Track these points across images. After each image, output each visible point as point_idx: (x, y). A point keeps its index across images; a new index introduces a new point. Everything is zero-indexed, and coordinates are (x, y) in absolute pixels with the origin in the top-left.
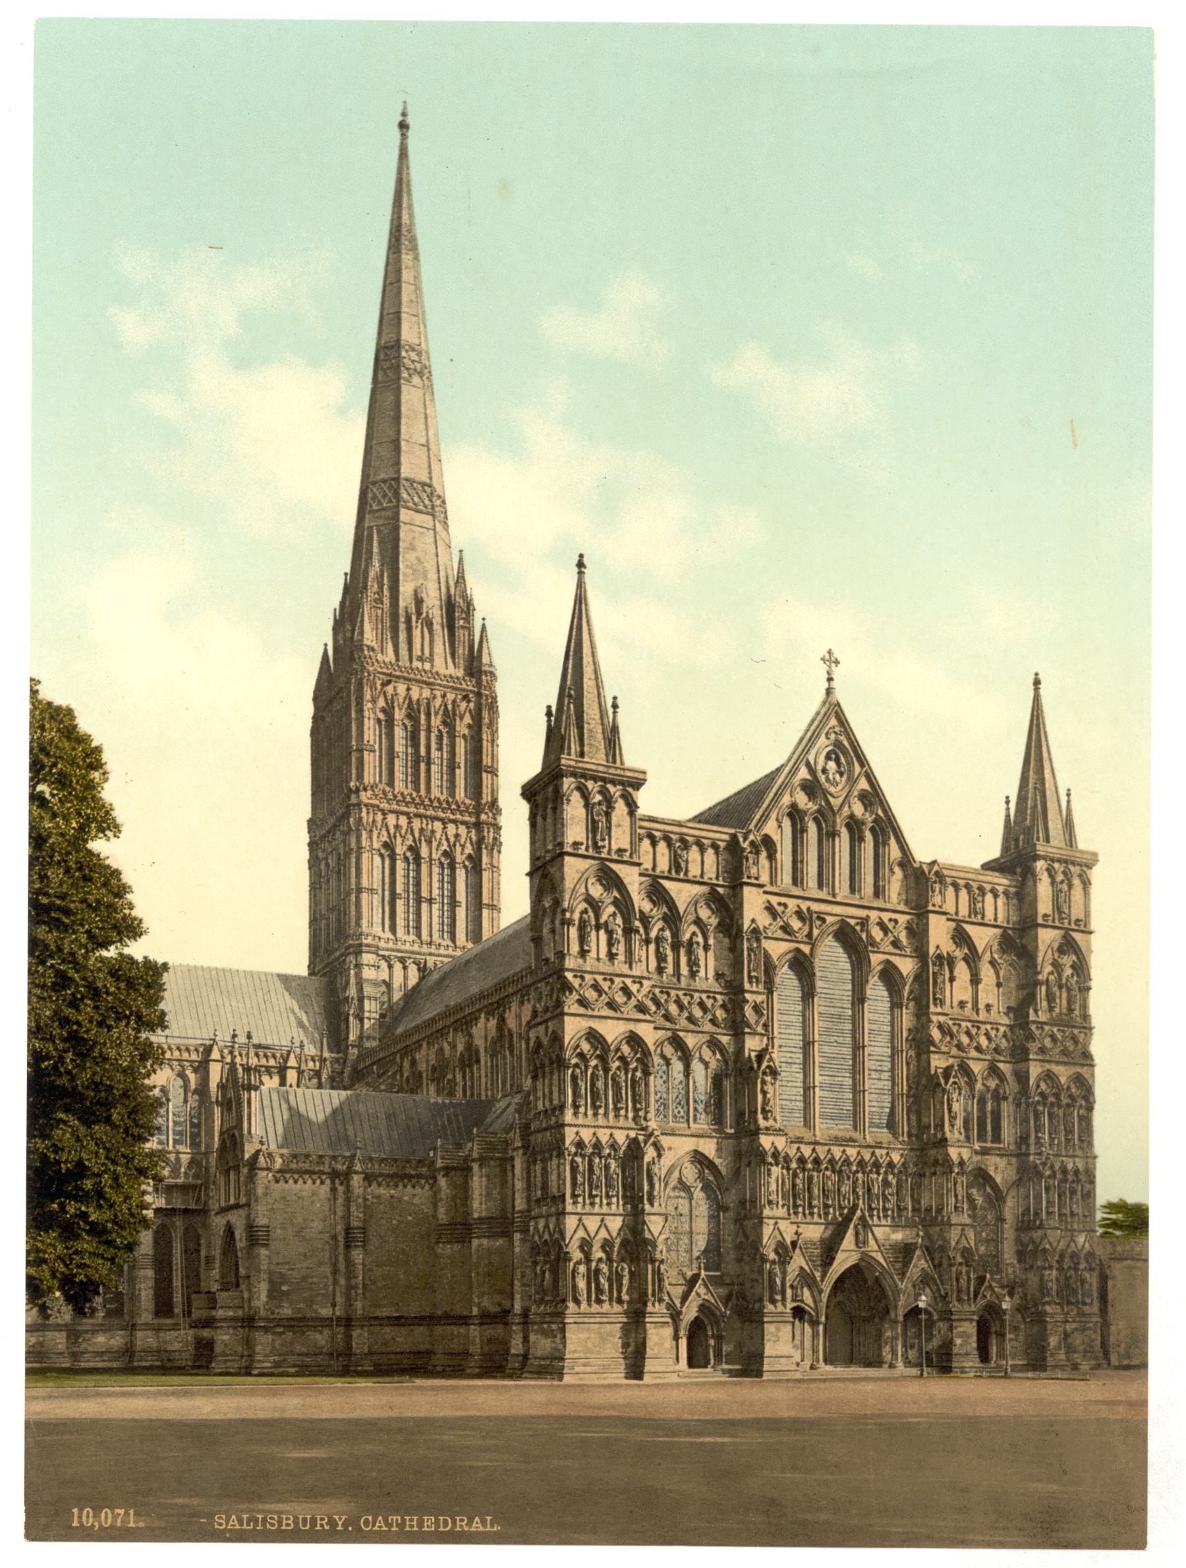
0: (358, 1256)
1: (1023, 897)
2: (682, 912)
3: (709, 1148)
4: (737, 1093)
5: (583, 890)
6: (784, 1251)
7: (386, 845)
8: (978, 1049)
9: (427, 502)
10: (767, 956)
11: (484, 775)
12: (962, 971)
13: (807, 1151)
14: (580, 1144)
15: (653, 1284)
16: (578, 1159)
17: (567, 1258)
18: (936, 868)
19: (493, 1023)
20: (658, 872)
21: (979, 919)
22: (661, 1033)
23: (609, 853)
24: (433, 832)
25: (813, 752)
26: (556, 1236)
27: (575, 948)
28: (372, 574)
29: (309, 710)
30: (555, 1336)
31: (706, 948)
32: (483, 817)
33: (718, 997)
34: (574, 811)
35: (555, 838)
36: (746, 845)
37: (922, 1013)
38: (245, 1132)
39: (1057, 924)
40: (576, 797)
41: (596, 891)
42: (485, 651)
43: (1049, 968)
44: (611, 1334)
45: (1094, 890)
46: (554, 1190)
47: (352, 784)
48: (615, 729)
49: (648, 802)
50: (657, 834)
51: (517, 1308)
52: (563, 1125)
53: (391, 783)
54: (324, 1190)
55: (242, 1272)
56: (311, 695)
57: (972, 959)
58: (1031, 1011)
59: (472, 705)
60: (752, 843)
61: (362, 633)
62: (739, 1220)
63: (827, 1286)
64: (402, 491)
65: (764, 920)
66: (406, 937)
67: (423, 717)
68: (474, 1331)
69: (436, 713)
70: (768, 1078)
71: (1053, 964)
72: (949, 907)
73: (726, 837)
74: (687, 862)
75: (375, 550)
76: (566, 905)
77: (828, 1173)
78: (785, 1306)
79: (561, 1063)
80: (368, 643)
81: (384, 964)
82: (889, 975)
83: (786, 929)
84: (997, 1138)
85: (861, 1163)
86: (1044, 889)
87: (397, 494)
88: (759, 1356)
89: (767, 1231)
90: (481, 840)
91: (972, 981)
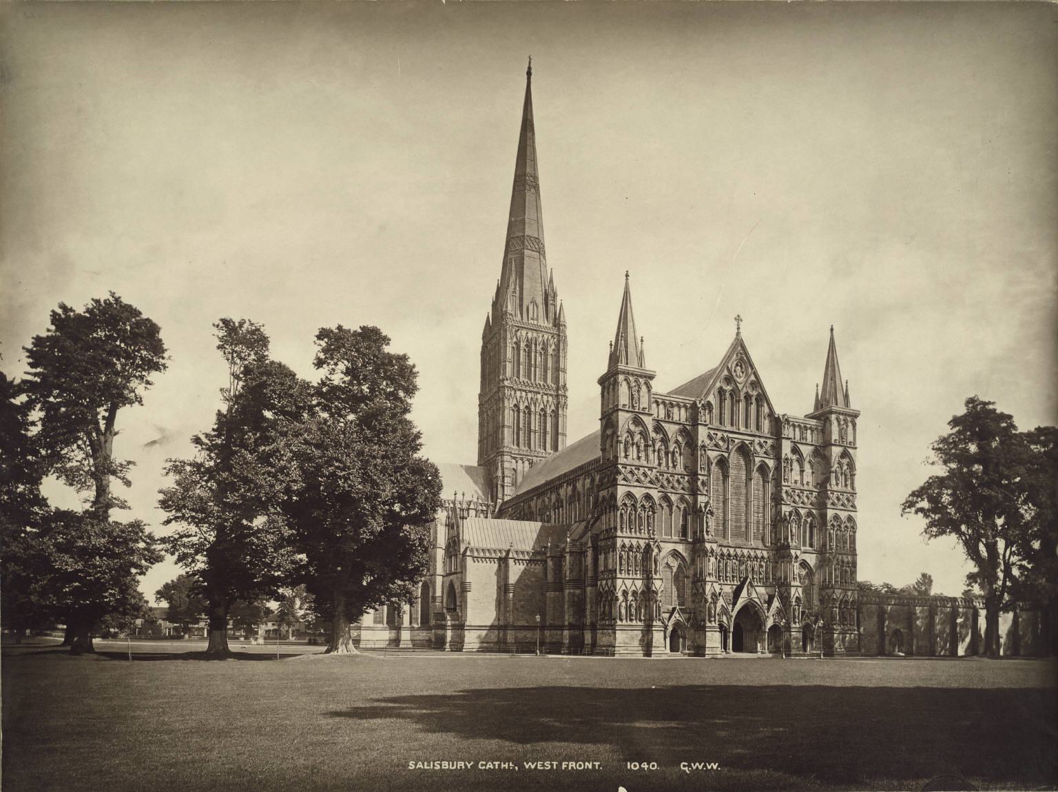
1: (824, 431)
2: (670, 437)
3: (680, 548)
4: (694, 521)
5: (627, 427)
6: (715, 596)
7: (515, 405)
8: (803, 503)
9: (537, 246)
10: (708, 458)
11: (561, 373)
12: (796, 466)
14: (624, 546)
15: (656, 613)
16: (623, 553)
17: (617, 599)
18: (786, 417)
19: (570, 488)
20: (660, 418)
21: (804, 441)
22: (661, 494)
23: (639, 409)
24: (537, 399)
26: (612, 588)
28: (511, 280)
29: (480, 343)
30: (611, 636)
31: (680, 455)
32: (560, 392)
33: (686, 478)
34: (623, 390)
35: (614, 403)
36: (699, 406)
37: (778, 485)
39: (841, 444)
40: (624, 384)
41: (632, 428)
42: (562, 315)
43: (836, 465)
44: (637, 635)
46: (610, 567)
48: (642, 352)
49: (661, 386)
50: (660, 401)
51: (588, 622)
52: (617, 537)
53: (518, 377)
55: (458, 604)
56: (481, 337)
57: (801, 461)
58: (828, 485)
60: (703, 405)
61: (507, 307)
62: (694, 583)
63: (734, 614)
64: (526, 241)
65: (707, 442)
67: (533, 346)
68: (566, 633)
69: (539, 344)
70: (709, 516)
71: (838, 463)
72: (791, 436)
73: (691, 402)
75: (513, 269)
76: (619, 433)
78: (715, 623)
79: (615, 507)
80: (510, 312)
81: (514, 461)
82: (763, 469)
83: (716, 445)
85: (749, 557)
86: (835, 428)
87: (523, 242)
89: (708, 587)
90: (558, 403)
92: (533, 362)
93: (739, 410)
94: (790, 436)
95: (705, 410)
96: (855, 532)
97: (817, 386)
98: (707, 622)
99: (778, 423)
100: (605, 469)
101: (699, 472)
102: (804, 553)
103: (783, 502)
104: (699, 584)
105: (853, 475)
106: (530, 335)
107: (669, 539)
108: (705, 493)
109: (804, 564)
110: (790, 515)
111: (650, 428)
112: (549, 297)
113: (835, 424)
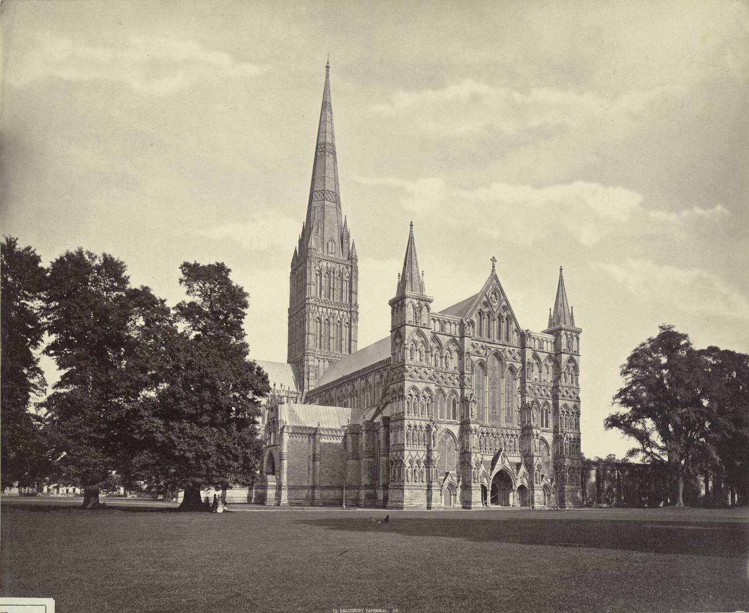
0: (318, 463)
5: (412, 338)
9: (334, 198)
10: (472, 361)
11: (353, 294)
12: (536, 368)
13: (484, 430)
14: (410, 426)
16: (409, 431)
19: (363, 382)
21: (542, 350)
25: (488, 292)
26: (400, 458)
27: (409, 358)
29: (290, 270)
32: (352, 309)
37: (523, 382)
38: (279, 419)
41: (416, 338)
42: (354, 251)
45: (580, 341)
47: (307, 297)
50: (436, 318)
54: (306, 440)
57: (539, 364)
59: (350, 270)
61: (311, 244)
63: (492, 477)
66: (325, 351)
69: (336, 273)
71: (566, 366)
74: (445, 328)
76: (406, 342)
77: (491, 437)
79: (402, 397)
80: (314, 247)
84: (547, 426)
86: (564, 340)
88: (470, 502)
89: (473, 457)
91: (539, 372)
92: (332, 286)
93: (494, 327)
94: (531, 346)
95: (469, 326)
96: (579, 417)
97: (550, 310)
98: (472, 483)
99: (524, 336)
100: (395, 368)
101: (465, 372)
102: (542, 431)
103: (526, 394)
104: (466, 455)
105: (577, 375)
106: (329, 265)
107: (443, 421)
108: (470, 387)
109: (543, 440)
110: (532, 405)
111: (429, 338)
112: (344, 237)
113: (564, 337)
